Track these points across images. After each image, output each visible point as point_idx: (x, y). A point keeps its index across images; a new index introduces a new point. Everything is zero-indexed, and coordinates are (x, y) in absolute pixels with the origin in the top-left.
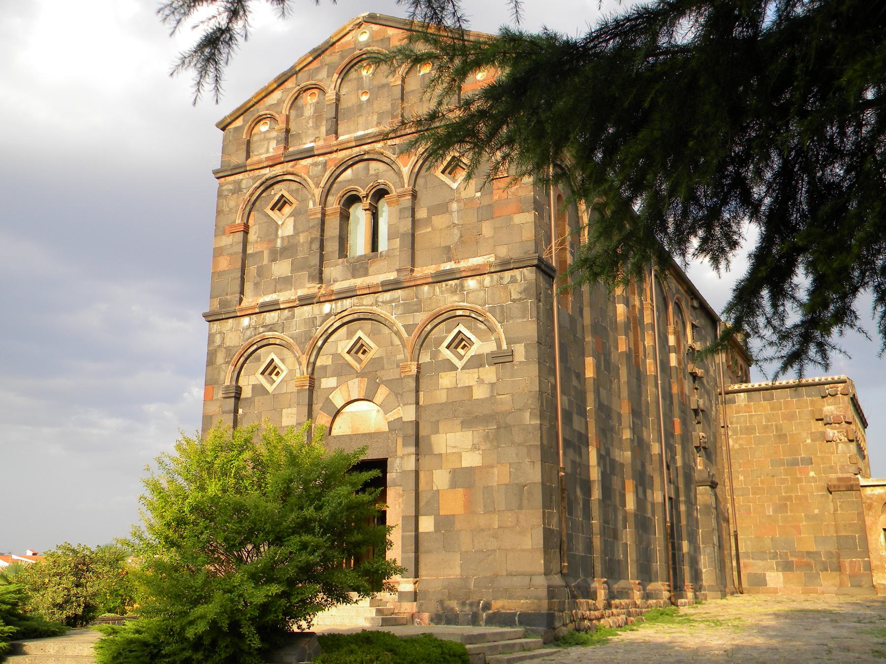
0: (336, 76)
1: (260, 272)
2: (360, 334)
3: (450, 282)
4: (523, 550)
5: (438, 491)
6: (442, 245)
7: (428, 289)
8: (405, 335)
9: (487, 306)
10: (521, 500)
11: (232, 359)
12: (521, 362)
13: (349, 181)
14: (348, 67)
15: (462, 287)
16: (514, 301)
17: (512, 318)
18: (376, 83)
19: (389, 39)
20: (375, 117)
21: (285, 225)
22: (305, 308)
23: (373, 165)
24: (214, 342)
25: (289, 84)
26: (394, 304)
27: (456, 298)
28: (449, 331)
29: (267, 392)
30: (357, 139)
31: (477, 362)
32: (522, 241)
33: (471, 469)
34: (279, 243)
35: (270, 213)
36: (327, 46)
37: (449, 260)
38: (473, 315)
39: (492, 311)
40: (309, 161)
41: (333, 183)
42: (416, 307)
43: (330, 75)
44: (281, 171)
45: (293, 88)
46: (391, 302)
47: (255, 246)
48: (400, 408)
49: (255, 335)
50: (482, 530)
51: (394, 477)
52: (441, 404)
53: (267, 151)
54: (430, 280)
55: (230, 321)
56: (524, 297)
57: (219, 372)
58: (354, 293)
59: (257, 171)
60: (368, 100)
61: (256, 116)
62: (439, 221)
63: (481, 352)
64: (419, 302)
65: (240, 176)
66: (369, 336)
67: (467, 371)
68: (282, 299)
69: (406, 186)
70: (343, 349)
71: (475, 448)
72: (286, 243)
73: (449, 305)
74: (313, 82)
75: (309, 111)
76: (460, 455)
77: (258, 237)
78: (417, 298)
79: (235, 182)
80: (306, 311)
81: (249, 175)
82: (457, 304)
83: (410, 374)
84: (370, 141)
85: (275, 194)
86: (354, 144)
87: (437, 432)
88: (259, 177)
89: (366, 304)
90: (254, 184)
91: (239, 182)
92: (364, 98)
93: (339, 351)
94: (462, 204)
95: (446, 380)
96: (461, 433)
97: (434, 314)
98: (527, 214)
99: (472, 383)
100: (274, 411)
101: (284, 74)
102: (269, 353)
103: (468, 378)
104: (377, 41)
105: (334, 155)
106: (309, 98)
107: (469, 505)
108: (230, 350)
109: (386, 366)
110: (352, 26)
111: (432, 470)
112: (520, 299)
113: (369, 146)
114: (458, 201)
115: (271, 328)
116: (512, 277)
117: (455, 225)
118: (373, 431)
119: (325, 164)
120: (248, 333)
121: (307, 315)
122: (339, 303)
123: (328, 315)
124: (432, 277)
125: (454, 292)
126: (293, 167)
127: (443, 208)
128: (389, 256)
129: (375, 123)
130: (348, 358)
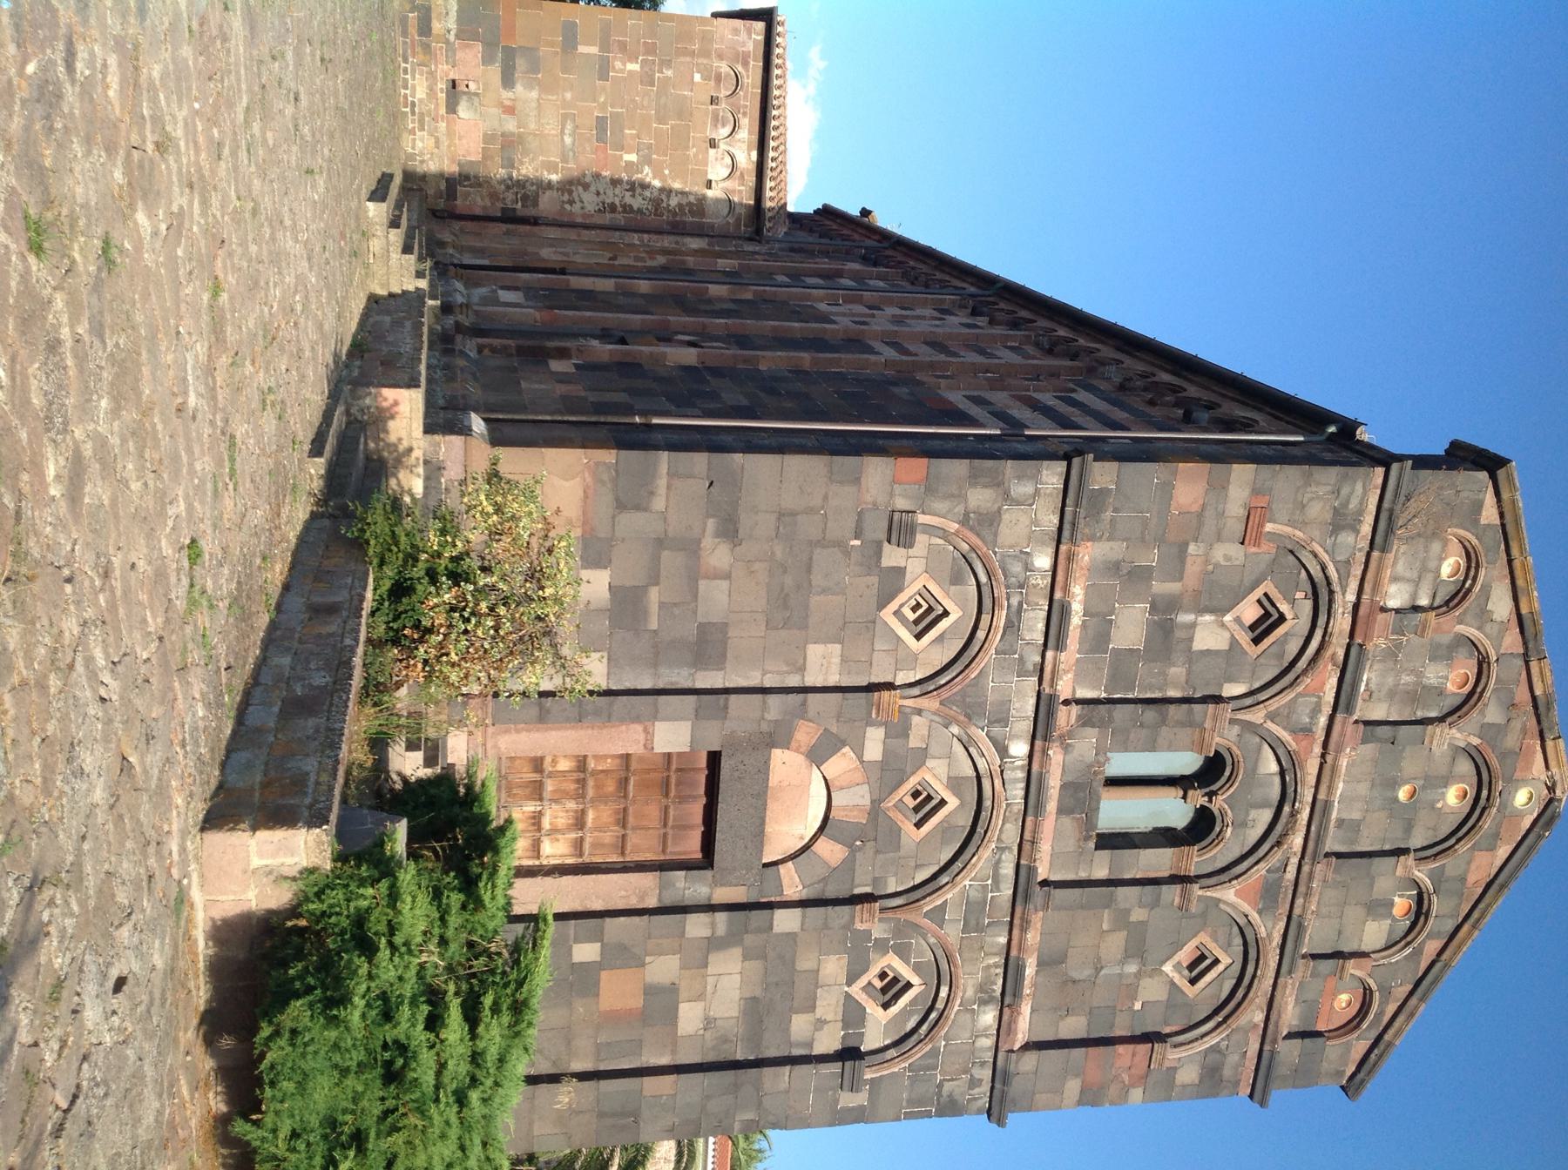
0: (1475, 741)
2: (953, 802)
3: (1000, 982)
4: (531, 1124)
5: (643, 965)
8: (929, 905)
10: (614, 1115)
11: (972, 529)
12: (837, 1101)
15: (983, 1002)
16: (940, 1086)
19: (1492, 848)
20: (1356, 816)
21: (1220, 630)
22: (1032, 701)
23: (1266, 816)
25: (1512, 641)
26: (989, 882)
27: (970, 993)
28: (917, 969)
29: (882, 605)
30: (1328, 805)
31: (853, 1015)
32: (1034, 1094)
33: (671, 1017)
35: (1258, 593)
36: (1545, 725)
37: (1041, 964)
38: (934, 1015)
39: (934, 1053)
40: (1329, 697)
42: (973, 923)
43: (1485, 730)
44: (1336, 630)
45: (1497, 650)
46: (996, 878)
47: (1199, 560)
48: (801, 887)
49: (1007, 587)
50: (569, 1043)
51: (678, 885)
52: (794, 963)
54: (1014, 953)
55: (1056, 521)
56: (942, 1100)
57: (953, 496)
58: (1030, 810)
59: (1359, 573)
60: (1396, 800)
61: (1483, 559)
62: (1115, 943)
63: (869, 1023)
64: (980, 928)
65: (1366, 529)
67: (842, 1001)
69: (1200, 893)
71: (709, 1022)
72: (1179, 634)
74: (1487, 694)
76: (700, 997)
77: (1217, 565)
79: (1361, 512)
81: (1360, 550)
83: (857, 919)
84: (1313, 828)
85: (1293, 602)
86: (1322, 796)
87: (746, 957)
89: (1005, 831)
90: (1335, 563)
92: (1403, 794)
93: (930, 763)
95: (833, 967)
96: (737, 998)
98: (1077, 1098)
99: (819, 1012)
100: (841, 623)
102: (962, 606)
103: (829, 1005)
104: (1499, 825)
105: (1318, 750)
106: (1462, 671)
107: (614, 1018)
108: (991, 525)
109: (881, 856)
111: (680, 952)
112: (939, 1094)
113: (1305, 822)
114: (1138, 975)
115: (1012, 626)
116: (981, 1081)
117: (1098, 970)
118: (768, 829)
119: (1307, 731)
120: (1016, 568)
121: (1017, 705)
122: (1021, 775)
123: (1003, 751)
124: (1018, 958)
125: (982, 988)
127: (1137, 948)
128: (1081, 854)
129: (1345, 816)
130: (911, 783)
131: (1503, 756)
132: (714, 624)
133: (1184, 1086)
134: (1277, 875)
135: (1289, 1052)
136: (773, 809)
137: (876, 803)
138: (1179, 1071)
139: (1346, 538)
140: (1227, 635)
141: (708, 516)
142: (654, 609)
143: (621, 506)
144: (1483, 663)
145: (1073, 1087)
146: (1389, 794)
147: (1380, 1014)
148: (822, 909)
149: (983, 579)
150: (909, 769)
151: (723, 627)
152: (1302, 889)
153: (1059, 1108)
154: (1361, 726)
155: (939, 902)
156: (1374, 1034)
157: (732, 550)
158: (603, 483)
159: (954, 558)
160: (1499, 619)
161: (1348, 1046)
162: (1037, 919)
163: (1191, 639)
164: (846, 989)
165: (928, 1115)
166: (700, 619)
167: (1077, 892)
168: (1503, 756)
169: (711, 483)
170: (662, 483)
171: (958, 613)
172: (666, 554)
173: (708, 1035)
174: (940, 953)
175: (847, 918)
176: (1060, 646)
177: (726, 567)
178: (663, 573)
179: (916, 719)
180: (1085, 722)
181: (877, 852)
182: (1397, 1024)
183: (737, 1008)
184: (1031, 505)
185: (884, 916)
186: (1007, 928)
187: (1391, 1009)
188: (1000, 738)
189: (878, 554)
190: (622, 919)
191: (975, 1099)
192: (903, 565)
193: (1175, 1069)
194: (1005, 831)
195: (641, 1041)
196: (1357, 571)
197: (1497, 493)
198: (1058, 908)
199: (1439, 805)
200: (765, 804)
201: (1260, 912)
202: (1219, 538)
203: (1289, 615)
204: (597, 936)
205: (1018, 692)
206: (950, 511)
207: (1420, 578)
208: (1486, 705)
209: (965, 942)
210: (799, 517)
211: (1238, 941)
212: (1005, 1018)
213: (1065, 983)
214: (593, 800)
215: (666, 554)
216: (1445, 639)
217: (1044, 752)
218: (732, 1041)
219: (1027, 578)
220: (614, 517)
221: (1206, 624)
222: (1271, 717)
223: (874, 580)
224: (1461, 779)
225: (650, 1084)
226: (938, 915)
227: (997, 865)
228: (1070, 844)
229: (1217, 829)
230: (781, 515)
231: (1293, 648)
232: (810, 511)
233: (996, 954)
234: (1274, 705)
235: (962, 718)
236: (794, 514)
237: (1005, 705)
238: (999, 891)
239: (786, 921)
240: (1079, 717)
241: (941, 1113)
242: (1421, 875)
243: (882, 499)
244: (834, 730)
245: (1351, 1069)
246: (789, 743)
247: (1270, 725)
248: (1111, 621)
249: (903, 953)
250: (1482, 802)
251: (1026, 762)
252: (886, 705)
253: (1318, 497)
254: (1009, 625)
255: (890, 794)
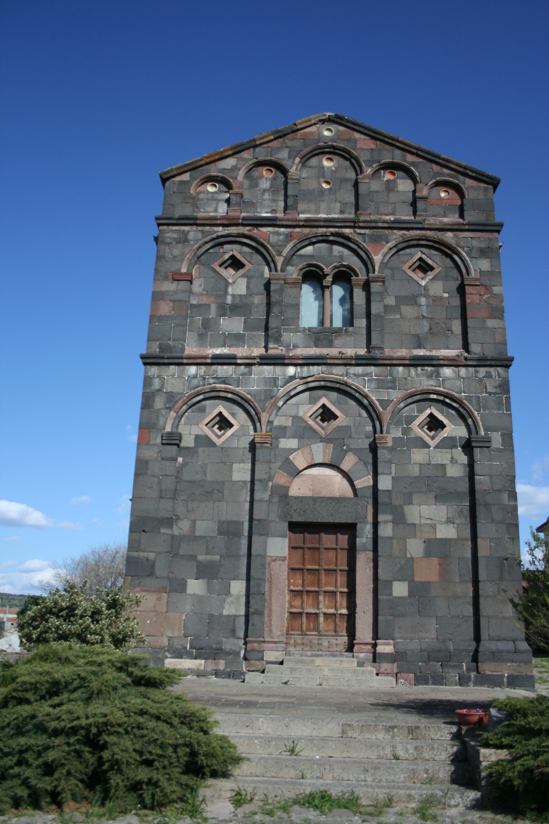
0: (298, 160)
1: (207, 324)
3: (426, 368)
4: (505, 618)
5: (412, 558)
6: (412, 333)
7: (403, 370)
9: (463, 394)
11: (174, 405)
12: (498, 450)
13: (311, 256)
14: (310, 155)
15: (438, 375)
16: (490, 394)
17: (488, 408)
18: (338, 175)
19: (355, 141)
20: (338, 205)
21: (237, 283)
22: (265, 367)
24: (151, 385)
25: (246, 155)
26: (366, 378)
27: (432, 382)
28: (421, 411)
29: (213, 445)
33: (445, 542)
34: (229, 300)
36: (289, 131)
37: (419, 347)
38: (447, 400)
40: (270, 229)
41: (293, 255)
42: (390, 385)
47: (201, 298)
49: (204, 385)
53: (216, 211)
54: (407, 362)
55: (172, 367)
56: (499, 392)
58: (324, 361)
60: (330, 189)
62: (408, 311)
63: (453, 434)
64: (394, 381)
65: (187, 228)
66: (334, 405)
67: (440, 450)
68: (239, 355)
69: (376, 273)
70: (305, 413)
71: (450, 521)
72: (237, 301)
73: (425, 388)
75: (265, 184)
76: (433, 527)
77: (204, 290)
78: (391, 376)
80: (268, 371)
81: (197, 229)
82: (433, 388)
84: (339, 224)
85: (224, 253)
87: (410, 503)
88: (210, 233)
89: (337, 373)
91: (186, 233)
93: (301, 414)
94: (431, 301)
96: (435, 507)
97: (410, 393)
98: (499, 320)
101: (242, 145)
102: (218, 405)
105: (297, 230)
106: (264, 172)
107: (444, 574)
108: (173, 396)
109: (353, 435)
110: (317, 120)
112: (495, 393)
113: (337, 230)
114: (427, 296)
115: (224, 381)
116: (487, 372)
118: (337, 495)
120: (195, 382)
122: (305, 368)
123: (292, 378)
125: (430, 376)
126: (249, 231)
127: (412, 300)
129: (338, 210)
130: (311, 422)
131: (306, 145)
132: (219, 528)
133: (492, 266)
134: (367, 238)
135: (471, 217)
136: (325, 493)
137: (322, 440)
138: (482, 270)
139: (191, 236)
140: (240, 279)
141: (159, 532)
142: (208, 557)
143: (152, 574)
144: (260, 164)
145: (491, 323)
146: (327, 192)
147: (449, 175)
148: (379, 465)
149: (201, 397)
150: (304, 425)
151: (221, 523)
152: (373, 225)
153: (505, 329)
154: (287, 212)
155: (377, 403)
156: (461, 178)
157: (181, 520)
158: (140, 583)
159: (192, 412)
160: (236, 162)
161: (469, 188)
162: (388, 352)
163: (240, 296)
164: (432, 448)
165: (508, 399)
166: (216, 534)
167: (373, 334)
168: (306, 145)
169: (144, 531)
170: (142, 554)
171: (222, 408)
172: (181, 552)
173: (457, 521)
174: (410, 400)
175: (384, 451)
176: (234, 357)
177: (189, 522)
178: (191, 553)
179: (276, 423)
180: (278, 340)
181: (351, 437)
182: (454, 166)
183: (441, 507)
184: (164, 378)
185: (385, 431)
186: (393, 368)
187: (446, 171)
188: (284, 381)
189: (187, 448)
190: (379, 571)
191: (499, 374)
192: (194, 436)
193: (481, 271)
194: (337, 373)
195: (459, 558)
196: (207, 228)
197: (174, 176)
198: (383, 342)
199: (334, 169)
200: (320, 498)
201: (388, 242)
202: (191, 292)
203: (231, 253)
204: (389, 583)
205: (260, 374)
206: (164, 416)
207: (216, 200)
208: (279, 159)
209: (401, 388)
210: (163, 488)
211: (408, 251)
212: (446, 363)
213: (431, 334)
214: (319, 587)
215: (181, 552)
216: (247, 183)
217: (291, 358)
218: (462, 508)
219: (201, 376)
220: (157, 577)
221: (233, 290)
222: (280, 254)
223: (200, 450)
224: (321, 161)
225: (483, 552)
226: (384, 403)
227: (357, 375)
228: (350, 339)
229: (344, 269)
230: (161, 497)
231: (246, 249)
232: (160, 482)
233: (409, 371)
234: (274, 253)
235: (272, 401)
236: (161, 491)
237: (266, 381)
238: (372, 373)
239: (385, 483)
240: (274, 343)
241: (507, 391)
242: (369, 171)
243: (156, 449)
244: (280, 464)
245: (482, 185)
246: (286, 487)
247: (285, 253)
248: (229, 334)
249: (410, 420)
250: (332, 150)
251: (298, 367)
252: (263, 439)
253: (171, 252)
254: (224, 382)
255: (317, 433)
